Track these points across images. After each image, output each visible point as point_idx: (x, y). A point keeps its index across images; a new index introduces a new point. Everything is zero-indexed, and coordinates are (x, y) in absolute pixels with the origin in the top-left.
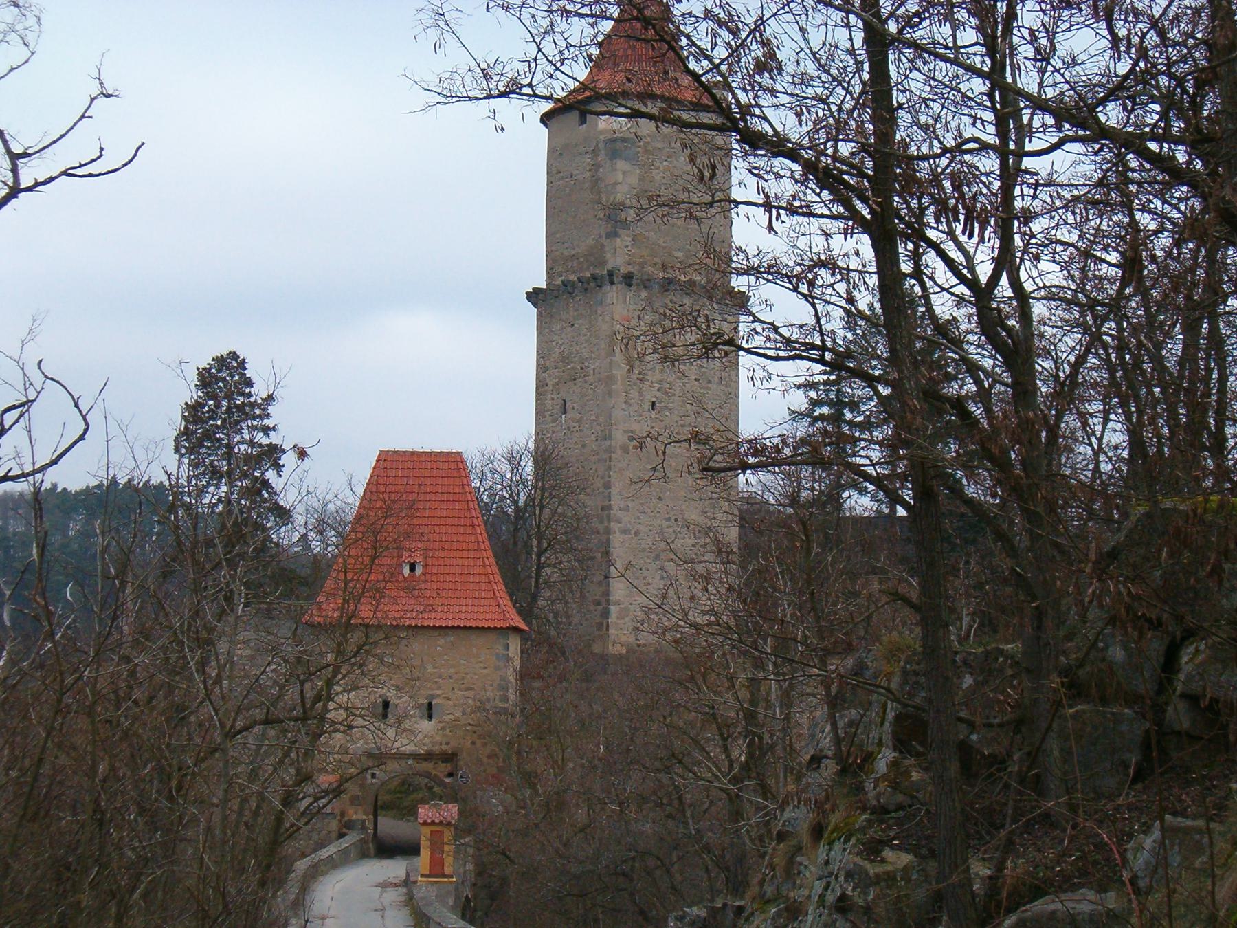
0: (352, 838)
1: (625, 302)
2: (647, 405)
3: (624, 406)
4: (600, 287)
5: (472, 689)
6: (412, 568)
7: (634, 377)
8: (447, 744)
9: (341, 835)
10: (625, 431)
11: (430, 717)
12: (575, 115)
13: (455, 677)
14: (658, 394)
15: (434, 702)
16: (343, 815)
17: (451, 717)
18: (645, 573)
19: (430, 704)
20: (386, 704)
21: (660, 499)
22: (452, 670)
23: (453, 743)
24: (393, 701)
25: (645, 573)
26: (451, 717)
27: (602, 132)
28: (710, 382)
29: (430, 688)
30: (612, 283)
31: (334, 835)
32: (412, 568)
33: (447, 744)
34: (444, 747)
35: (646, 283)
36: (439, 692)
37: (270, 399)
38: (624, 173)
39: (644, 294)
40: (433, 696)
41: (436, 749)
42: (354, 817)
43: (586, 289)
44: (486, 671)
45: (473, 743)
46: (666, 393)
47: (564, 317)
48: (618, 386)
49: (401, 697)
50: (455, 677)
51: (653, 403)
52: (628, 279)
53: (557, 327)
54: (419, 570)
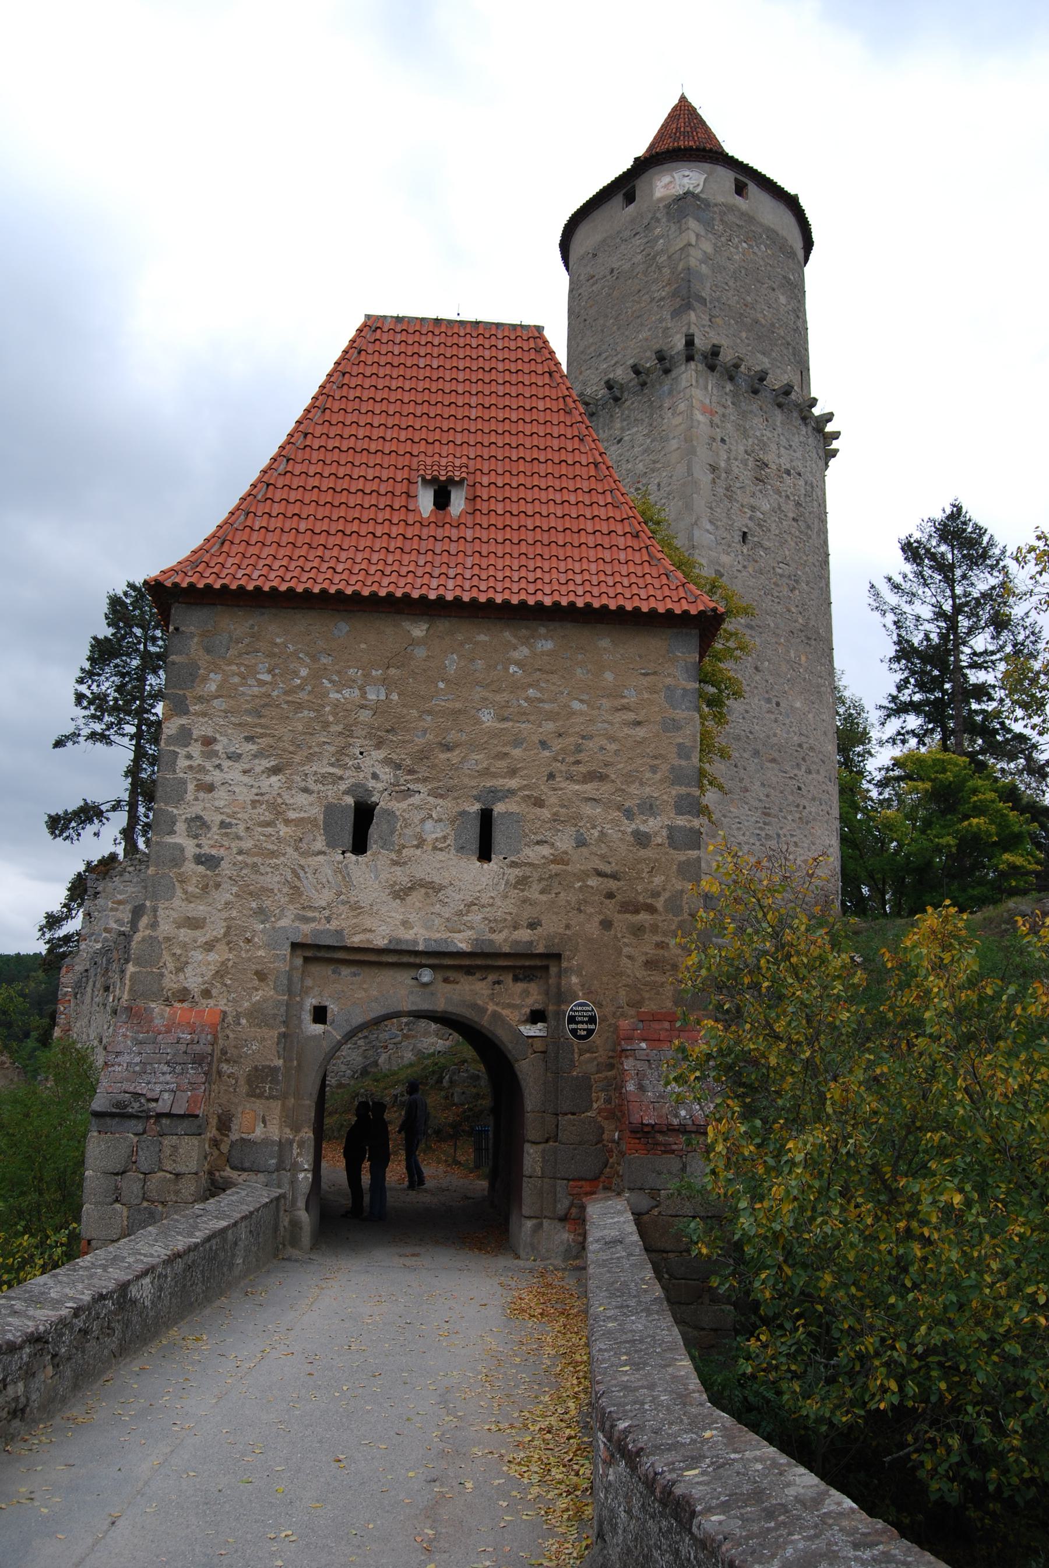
0: (247, 1196)
1: (706, 388)
2: (738, 538)
3: (709, 527)
4: (667, 371)
5: (602, 778)
6: (442, 501)
7: (721, 491)
9: (215, 1187)
11: (485, 854)
12: (618, 200)
14: (751, 524)
15: (499, 808)
16: (224, 1124)
17: (545, 851)
19: (486, 817)
20: (364, 814)
21: (756, 668)
22: (550, 726)
23: (552, 926)
24: (383, 802)
26: (545, 851)
27: (661, 200)
29: (486, 773)
30: (690, 358)
31: (188, 1188)
32: (442, 501)
33: (532, 926)
34: (524, 935)
35: (731, 373)
36: (513, 783)
39: (729, 387)
41: (502, 940)
42: (259, 1133)
43: (643, 384)
44: (641, 732)
45: (607, 924)
48: (700, 503)
49: (408, 793)
50: (557, 745)
52: (712, 359)
54: (458, 503)
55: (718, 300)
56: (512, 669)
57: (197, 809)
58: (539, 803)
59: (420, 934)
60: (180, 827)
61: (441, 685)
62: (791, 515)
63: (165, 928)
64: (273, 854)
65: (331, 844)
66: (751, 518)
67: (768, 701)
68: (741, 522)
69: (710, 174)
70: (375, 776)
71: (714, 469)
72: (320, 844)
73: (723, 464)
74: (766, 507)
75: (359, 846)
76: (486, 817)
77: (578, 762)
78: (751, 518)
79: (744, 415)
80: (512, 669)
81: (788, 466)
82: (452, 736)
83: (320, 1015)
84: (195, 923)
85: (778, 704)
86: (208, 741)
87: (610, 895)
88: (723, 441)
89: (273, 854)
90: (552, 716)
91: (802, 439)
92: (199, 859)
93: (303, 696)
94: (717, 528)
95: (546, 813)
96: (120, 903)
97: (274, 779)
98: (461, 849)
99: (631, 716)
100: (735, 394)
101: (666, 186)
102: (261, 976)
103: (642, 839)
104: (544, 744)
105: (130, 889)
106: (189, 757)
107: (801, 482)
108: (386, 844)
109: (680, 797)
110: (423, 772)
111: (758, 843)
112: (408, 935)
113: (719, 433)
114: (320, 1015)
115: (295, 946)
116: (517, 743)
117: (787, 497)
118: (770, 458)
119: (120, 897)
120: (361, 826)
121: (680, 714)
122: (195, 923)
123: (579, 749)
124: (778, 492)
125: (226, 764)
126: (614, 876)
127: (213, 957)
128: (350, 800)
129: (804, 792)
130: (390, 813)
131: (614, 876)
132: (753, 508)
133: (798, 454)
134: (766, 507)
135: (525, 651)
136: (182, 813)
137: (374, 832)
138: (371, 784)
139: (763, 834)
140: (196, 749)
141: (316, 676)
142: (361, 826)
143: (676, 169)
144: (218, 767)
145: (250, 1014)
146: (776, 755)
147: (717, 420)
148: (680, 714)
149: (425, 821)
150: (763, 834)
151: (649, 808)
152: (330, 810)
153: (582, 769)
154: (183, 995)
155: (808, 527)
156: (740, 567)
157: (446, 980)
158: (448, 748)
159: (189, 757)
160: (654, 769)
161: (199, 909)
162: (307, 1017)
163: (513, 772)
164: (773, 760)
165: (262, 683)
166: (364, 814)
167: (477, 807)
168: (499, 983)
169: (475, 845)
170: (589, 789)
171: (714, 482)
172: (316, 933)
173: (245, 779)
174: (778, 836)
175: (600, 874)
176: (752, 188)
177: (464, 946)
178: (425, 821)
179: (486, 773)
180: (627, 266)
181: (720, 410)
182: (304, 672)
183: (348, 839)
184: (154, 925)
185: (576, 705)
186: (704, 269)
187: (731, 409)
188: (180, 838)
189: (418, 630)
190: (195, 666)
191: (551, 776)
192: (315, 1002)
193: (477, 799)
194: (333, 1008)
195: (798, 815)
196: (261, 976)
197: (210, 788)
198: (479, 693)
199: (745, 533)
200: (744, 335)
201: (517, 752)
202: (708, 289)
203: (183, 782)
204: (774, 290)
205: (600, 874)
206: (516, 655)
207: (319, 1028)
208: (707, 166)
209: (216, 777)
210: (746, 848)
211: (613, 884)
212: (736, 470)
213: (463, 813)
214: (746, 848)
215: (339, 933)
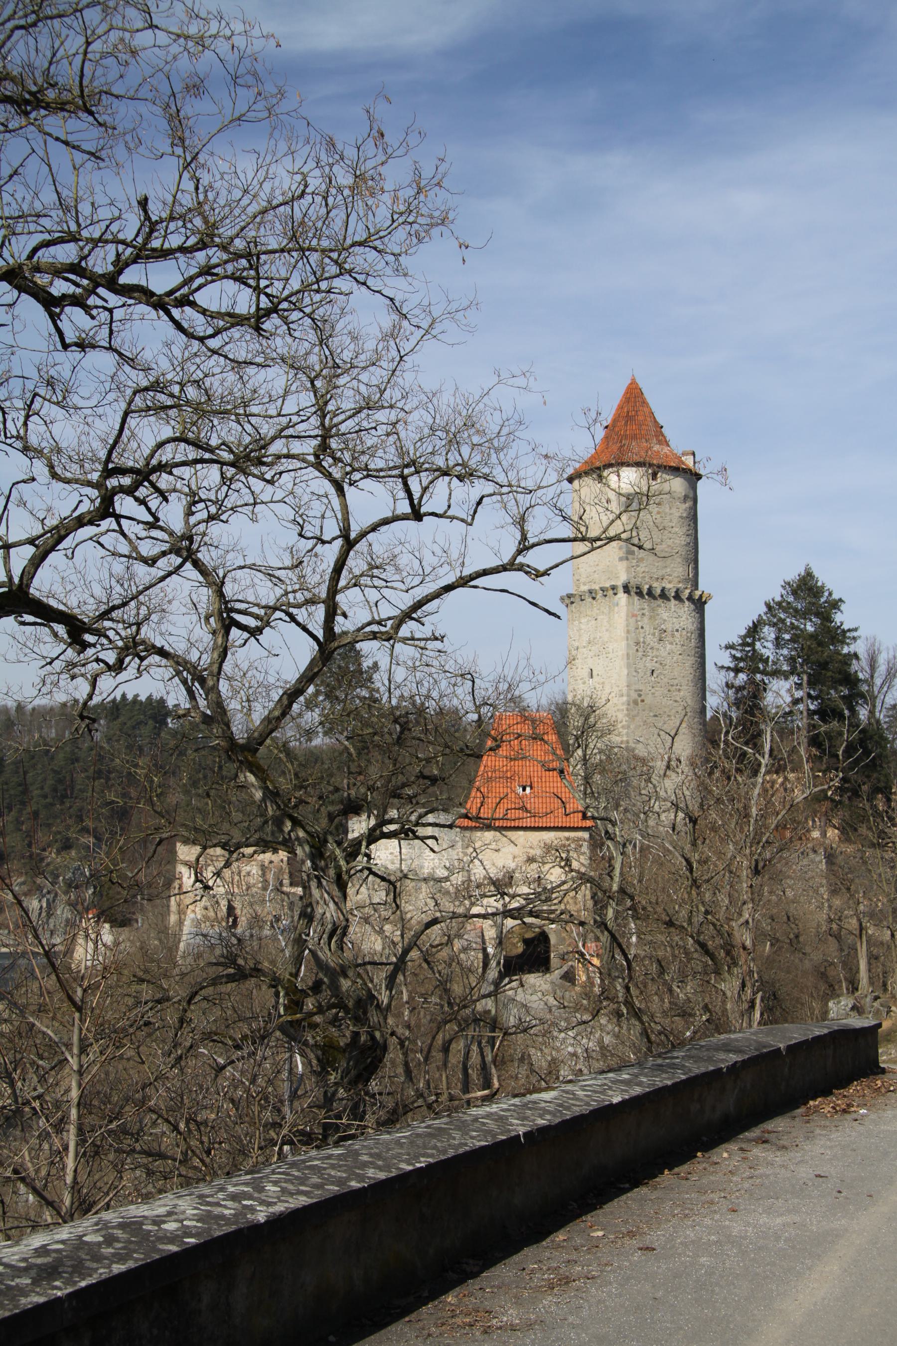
2: (649, 673)
4: (615, 594)
6: (524, 790)
7: (640, 654)
32: (524, 790)
47: (589, 613)
53: (583, 620)
68: (650, 665)
71: (637, 643)
79: (653, 610)
118: (668, 626)
124: (671, 643)
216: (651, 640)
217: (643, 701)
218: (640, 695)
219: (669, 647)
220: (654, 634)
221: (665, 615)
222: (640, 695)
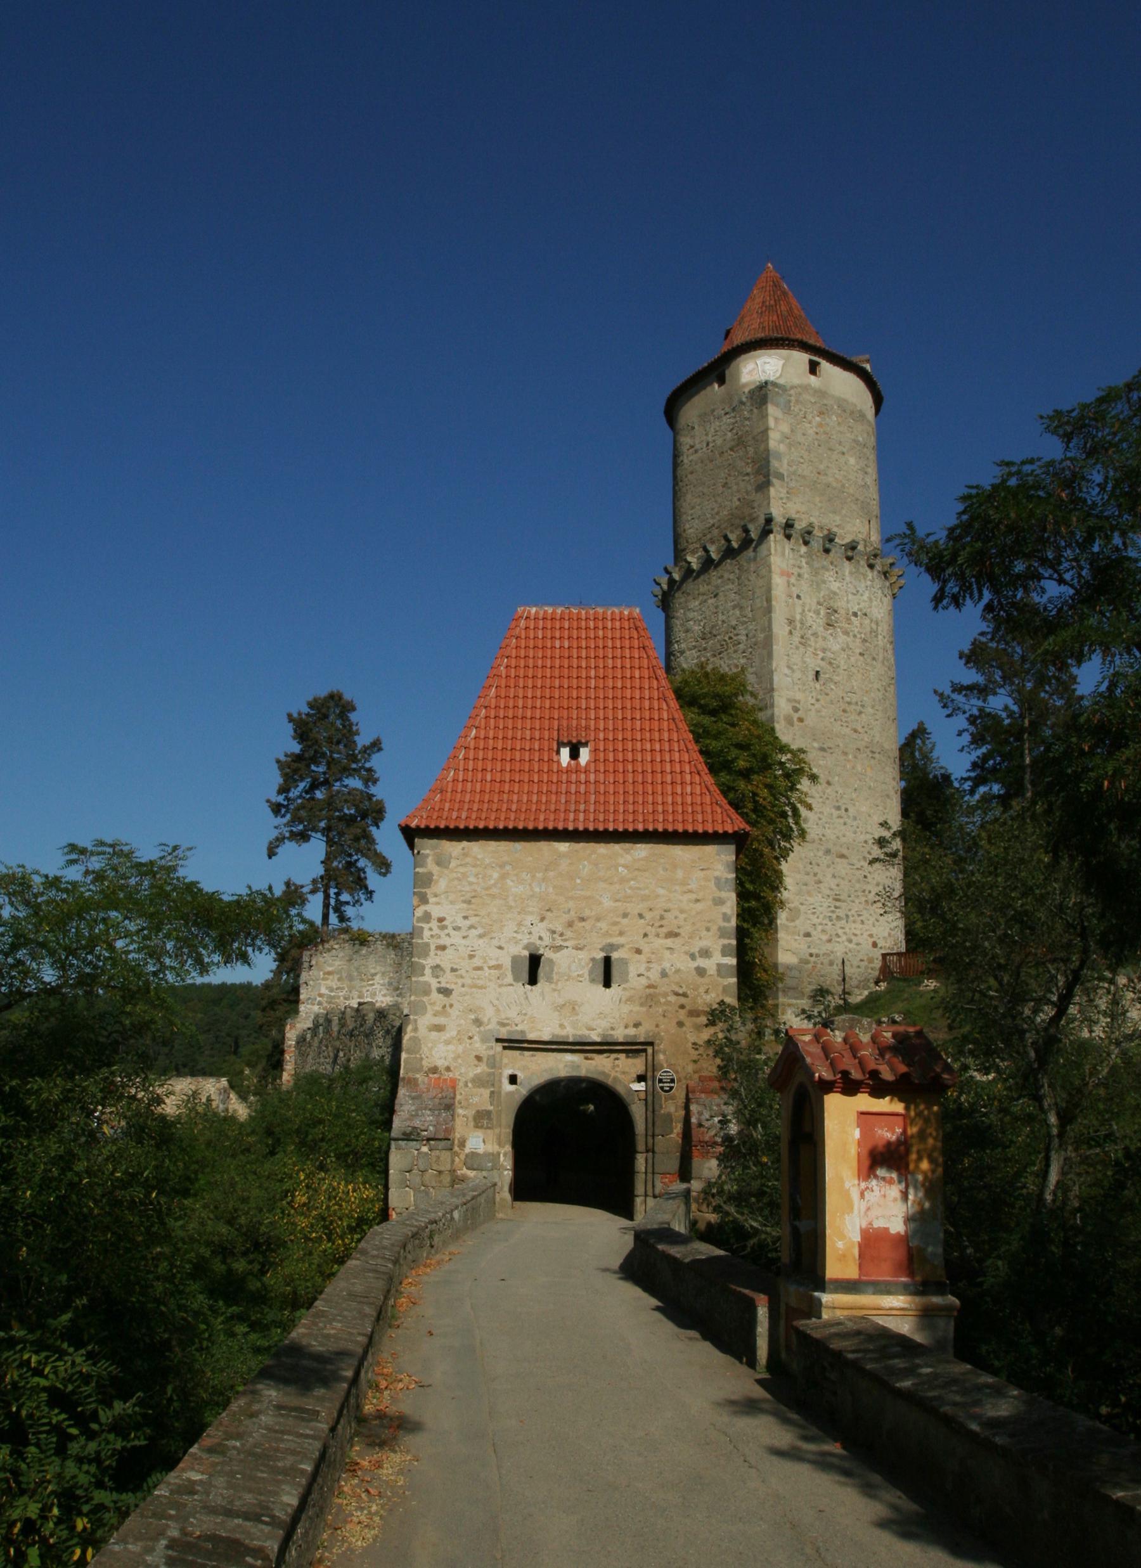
1: (783, 554)
2: (811, 675)
3: (786, 671)
5: (677, 935)
6: (574, 755)
7: (796, 639)
8: (636, 1025)
10: (789, 700)
11: (607, 984)
13: (648, 916)
14: (823, 663)
15: (615, 955)
18: (816, 869)
19: (607, 961)
20: (535, 961)
24: (548, 954)
25: (816, 869)
28: (874, 659)
32: (574, 755)
33: (636, 1025)
34: (632, 1031)
35: (806, 537)
37: (376, 746)
38: (776, 419)
39: (804, 549)
40: (613, 947)
41: (619, 1034)
44: (699, 906)
45: (680, 1024)
46: (830, 663)
51: (817, 672)
55: (794, 473)
56: (620, 869)
57: (438, 961)
58: (638, 951)
59: (570, 1032)
60: (428, 971)
61: (578, 881)
62: (858, 651)
63: (422, 1032)
64: (481, 987)
65: (516, 979)
66: (822, 659)
67: (838, 808)
68: (814, 663)
69: (787, 359)
70: (540, 938)
71: (791, 622)
72: (509, 978)
73: (798, 617)
74: (836, 648)
75: (533, 980)
76: (607, 961)
77: (661, 926)
78: (822, 659)
79: (815, 572)
80: (620, 869)
81: (855, 610)
82: (587, 913)
83: (513, 1079)
84: (439, 1028)
85: (846, 810)
86: (441, 920)
87: (682, 1007)
88: (798, 597)
89: (481, 987)
90: (645, 898)
91: (869, 583)
92: (441, 991)
93: (494, 891)
94: (793, 671)
95: (642, 958)
96: (329, 973)
97: (481, 941)
98: (592, 981)
99: (693, 896)
100: (809, 555)
101: (751, 372)
102: (479, 1058)
103: (701, 972)
104: (641, 916)
105: (337, 963)
106: (431, 929)
107: (867, 621)
108: (549, 979)
109: (724, 946)
110: (569, 934)
111: (830, 923)
112: (563, 1033)
113: (795, 591)
114: (513, 1079)
115: (498, 1040)
116: (625, 915)
117: (855, 636)
118: (840, 604)
119: (330, 969)
120: (533, 968)
121: (724, 894)
122: (439, 1028)
123: (662, 918)
124: (846, 633)
125: (453, 933)
126: (685, 995)
127: (451, 1047)
128: (526, 953)
129: (869, 879)
130: (551, 961)
131: (685, 995)
132: (824, 650)
133: (865, 597)
134: (836, 648)
135: (629, 857)
136: (429, 962)
137: (542, 972)
138: (538, 942)
139: (834, 916)
140: (434, 924)
141: (503, 877)
142: (533, 968)
143: (759, 357)
144: (448, 935)
145: (473, 1081)
146: (845, 851)
147: (793, 580)
148: (724, 894)
149: (571, 964)
150: (834, 916)
151: (706, 953)
152: (515, 960)
153: (664, 930)
154: (434, 1070)
155: (874, 659)
156: (813, 701)
157: (586, 1058)
158: (582, 919)
159: (431, 929)
160: (708, 929)
161: (441, 1020)
162: (505, 1081)
163: (621, 934)
164: (842, 856)
165: (471, 884)
166: (535, 961)
167: (602, 955)
168: (617, 1059)
169: (601, 978)
170: (669, 942)
171: (791, 633)
172: (509, 1032)
173: (463, 942)
174: (847, 916)
175: (677, 994)
176: (825, 365)
177: (598, 1040)
178: (571, 964)
179: (607, 934)
180: (719, 442)
181: (796, 571)
182: (496, 875)
183: (525, 975)
184: (415, 1030)
185: (661, 891)
186: (782, 448)
187: (806, 569)
188: (427, 977)
189: (563, 847)
190: (430, 874)
191: (645, 935)
192: (510, 1072)
193: (602, 950)
194: (521, 1076)
195: (864, 899)
196: (479, 1058)
197: (443, 948)
198: (602, 885)
199: (817, 672)
200: (817, 499)
201: (625, 921)
202: (785, 466)
203: (427, 945)
204: (843, 454)
205: (677, 994)
206: (622, 861)
207: (512, 1088)
208: (784, 352)
209: (445, 941)
210: (820, 928)
211: (683, 1000)
212: (810, 622)
213: (593, 959)
214: (820, 928)
215: (522, 1032)
216: (816, 622)
217: (801, 720)
218: (796, 710)
219: (842, 638)
220: (817, 613)
221: (835, 586)
222: (796, 710)
